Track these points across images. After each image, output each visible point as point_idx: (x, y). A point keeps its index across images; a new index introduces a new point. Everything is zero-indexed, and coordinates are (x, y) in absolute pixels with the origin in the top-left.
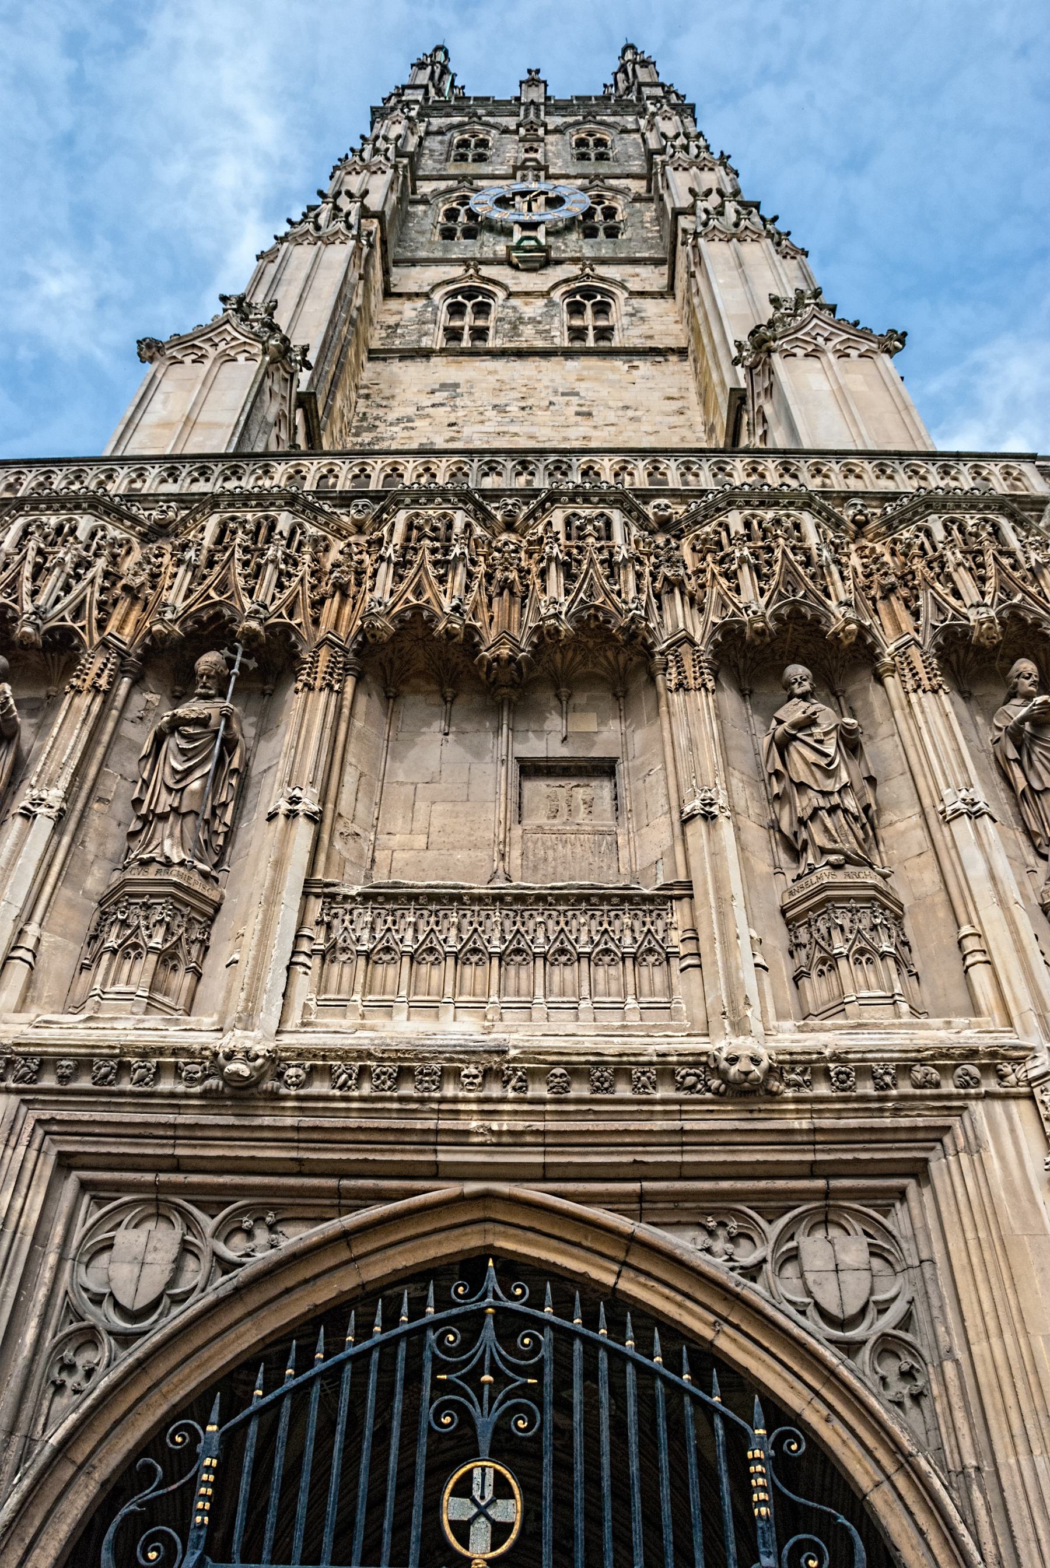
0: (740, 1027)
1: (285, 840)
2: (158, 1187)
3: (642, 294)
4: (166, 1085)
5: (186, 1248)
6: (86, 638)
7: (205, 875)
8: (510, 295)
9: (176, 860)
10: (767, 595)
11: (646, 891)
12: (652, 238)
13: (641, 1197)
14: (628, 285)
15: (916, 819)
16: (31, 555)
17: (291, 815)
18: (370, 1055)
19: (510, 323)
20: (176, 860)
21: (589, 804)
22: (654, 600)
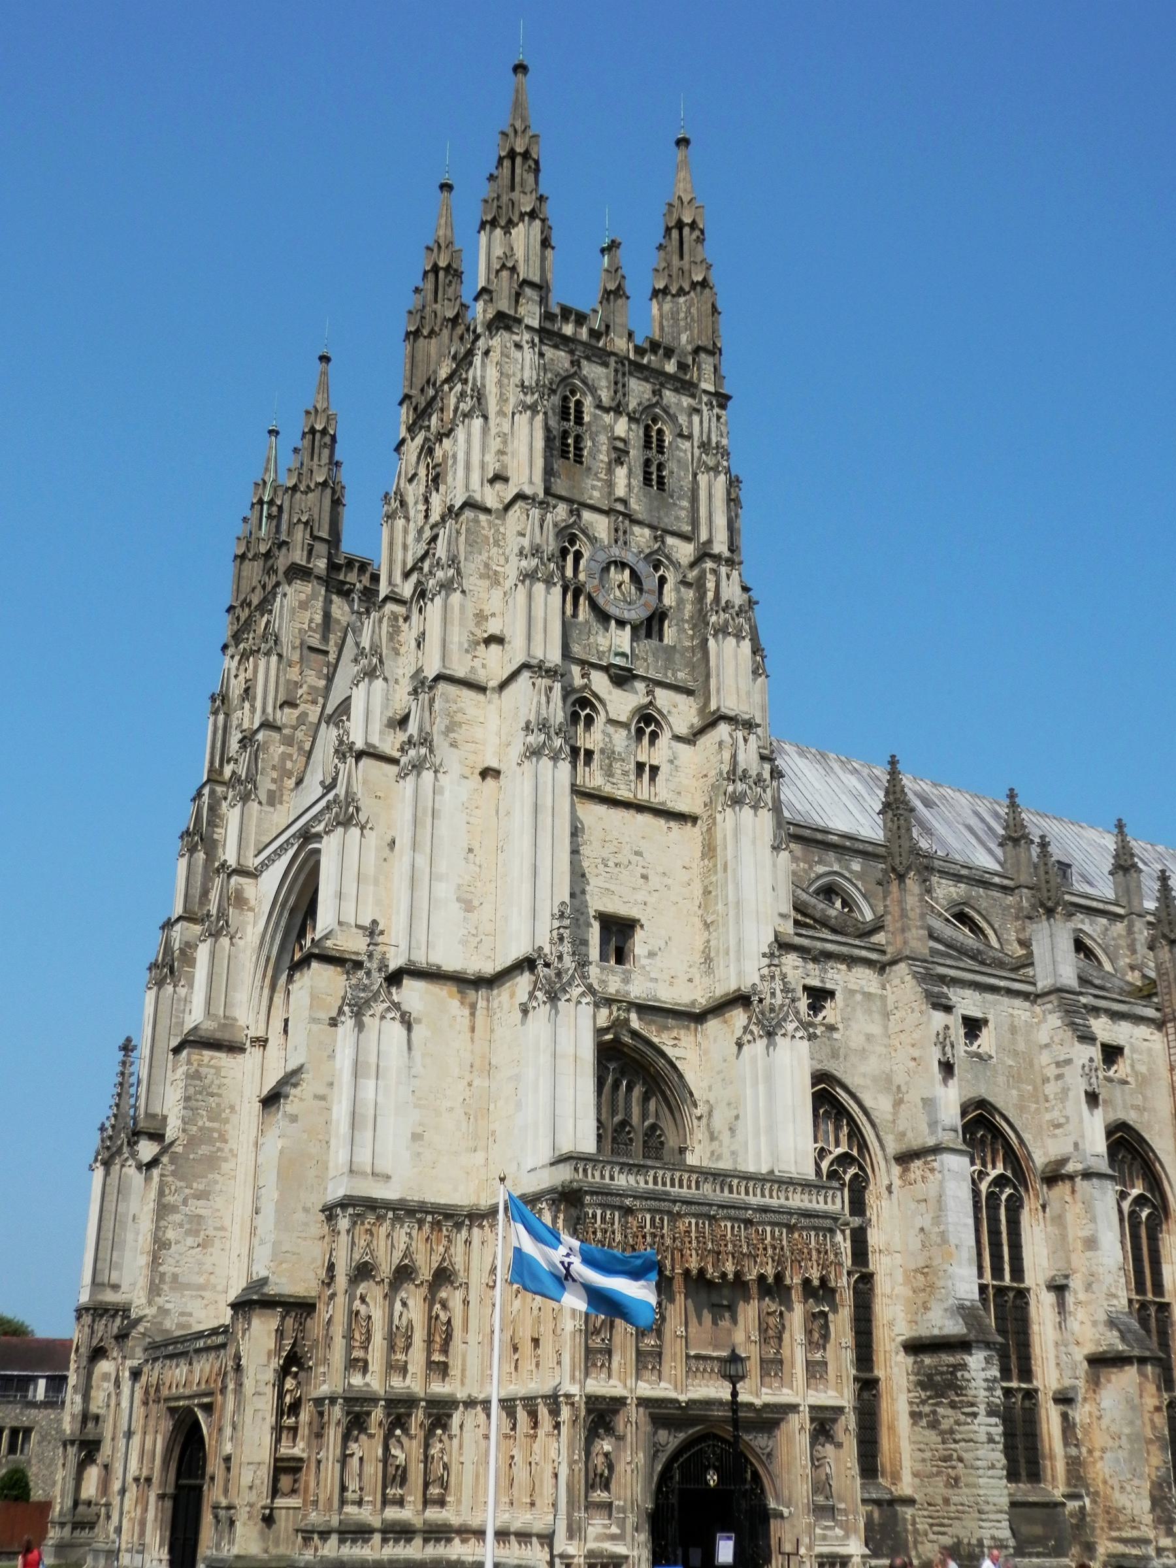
3: (677, 738)
8: (611, 721)
12: (687, 649)
14: (670, 719)
19: (609, 758)
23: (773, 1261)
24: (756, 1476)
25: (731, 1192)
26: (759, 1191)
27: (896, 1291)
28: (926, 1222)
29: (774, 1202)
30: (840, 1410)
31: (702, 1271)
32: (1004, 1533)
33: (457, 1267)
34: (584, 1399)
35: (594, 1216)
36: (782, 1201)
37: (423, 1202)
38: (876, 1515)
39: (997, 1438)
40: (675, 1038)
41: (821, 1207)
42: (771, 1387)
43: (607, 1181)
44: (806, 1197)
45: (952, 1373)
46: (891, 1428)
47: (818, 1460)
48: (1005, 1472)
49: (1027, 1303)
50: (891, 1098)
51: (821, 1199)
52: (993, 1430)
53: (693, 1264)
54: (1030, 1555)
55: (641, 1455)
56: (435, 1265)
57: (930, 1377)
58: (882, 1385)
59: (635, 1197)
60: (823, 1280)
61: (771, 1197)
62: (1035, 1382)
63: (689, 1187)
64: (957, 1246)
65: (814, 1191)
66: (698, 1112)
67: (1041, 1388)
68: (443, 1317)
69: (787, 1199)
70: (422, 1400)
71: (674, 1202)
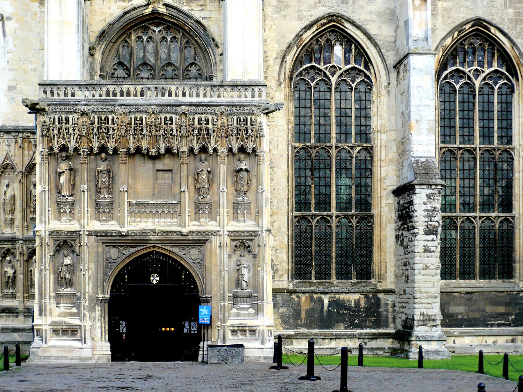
1: (124, 196)
11: (175, 202)
17: (124, 191)
21: (168, 177)
23: (199, 138)
24: (190, 276)
25: (170, 95)
26: (194, 94)
27: (390, 156)
28: (403, 107)
29: (206, 100)
31: (138, 150)
32: (435, 310)
34: (47, 233)
35: (54, 119)
38: (363, 303)
39: (432, 249)
40: (202, 5)
41: (249, 100)
42: (199, 221)
45: (408, 208)
46: (380, 246)
47: (239, 266)
48: (439, 271)
49: (512, 159)
50: (394, 26)
51: (249, 94)
52: (429, 244)
53: (132, 145)
54: (492, 325)
55: (93, 265)
57: (402, 211)
58: (376, 220)
60: (242, 150)
61: (205, 96)
62: (514, 212)
63: (136, 95)
64: (417, 121)
65: (242, 89)
66: (219, 51)
67: (517, 215)
69: (219, 96)
71: (121, 105)
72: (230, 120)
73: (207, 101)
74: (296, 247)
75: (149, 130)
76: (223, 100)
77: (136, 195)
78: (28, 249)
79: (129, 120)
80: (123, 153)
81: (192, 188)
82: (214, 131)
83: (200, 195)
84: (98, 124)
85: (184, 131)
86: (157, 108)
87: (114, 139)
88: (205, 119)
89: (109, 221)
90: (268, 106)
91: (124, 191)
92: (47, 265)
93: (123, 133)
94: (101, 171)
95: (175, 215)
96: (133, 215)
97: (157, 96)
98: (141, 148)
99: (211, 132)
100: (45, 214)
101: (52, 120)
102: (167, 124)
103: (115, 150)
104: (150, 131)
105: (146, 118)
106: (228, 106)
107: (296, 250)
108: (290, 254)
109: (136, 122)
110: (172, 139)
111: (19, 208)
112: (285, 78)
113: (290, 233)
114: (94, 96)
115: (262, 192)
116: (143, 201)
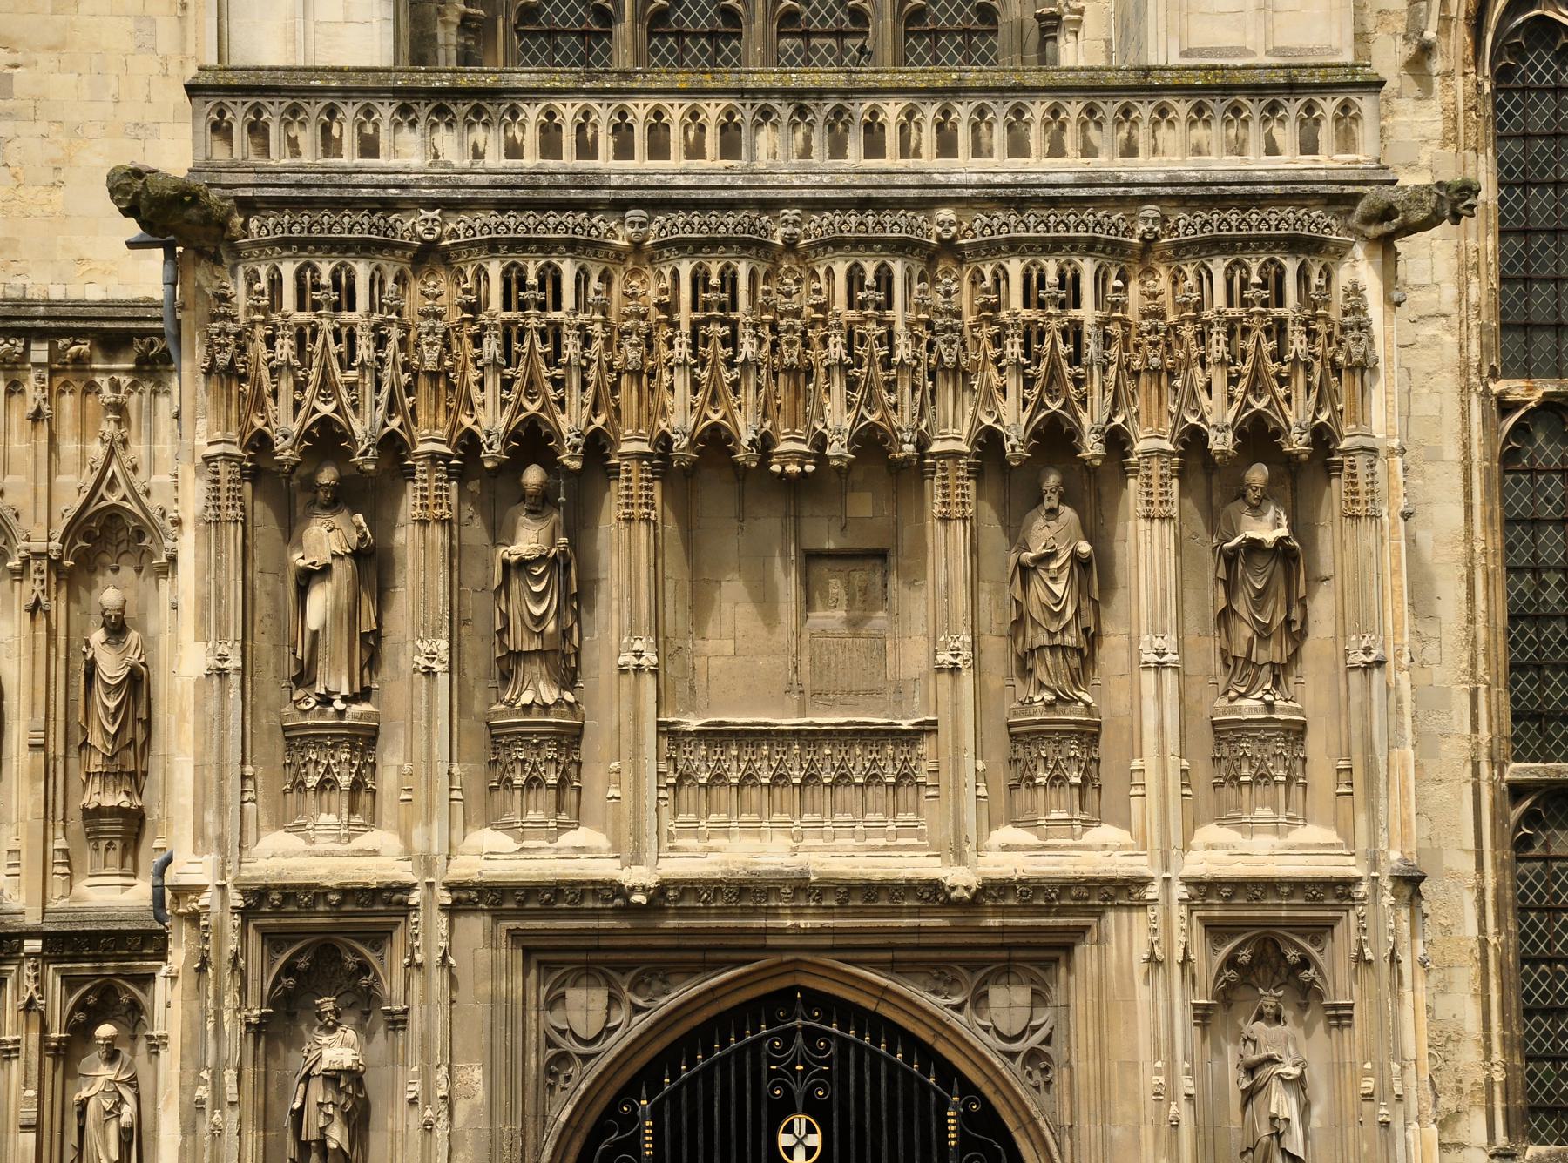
0: (959, 858)
1: (636, 694)
2: (587, 962)
4: (588, 904)
5: (611, 997)
6: (406, 437)
7: (569, 704)
9: (551, 702)
10: (1030, 408)
11: (905, 725)
13: (893, 961)
15: (1125, 638)
16: (330, 339)
18: (720, 881)
20: (551, 702)
22: (929, 384)
25: (874, 148)
26: (999, 136)
29: (1066, 168)
30: (1341, 889)
31: (715, 441)
33: (152, 504)
34: (236, 899)
36: (1107, 162)
37: (17, 304)
43: (349, 158)
44: (1213, 134)
56: (70, 502)
59: (450, 206)
61: (1057, 149)
68: (111, 666)
70: (32, 935)
71: (619, 206)
72: (1192, 281)
73: (1069, 178)
74: (1524, 961)
75: (769, 338)
76: (1148, 166)
77: (700, 683)
78: (70, 983)
79: (667, 284)
80: (634, 465)
81: (996, 649)
82: (1107, 340)
83: (1042, 686)
84: (507, 306)
85: (950, 343)
86: (817, 225)
87: (591, 390)
88: (1061, 276)
89: (562, 828)
90: (1387, 194)
91: (639, 669)
92: (230, 1076)
93: (631, 354)
94: (523, 565)
95: (907, 794)
96: (688, 794)
97: (806, 153)
98: (730, 438)
99: (1092, 348)
100: (221, 795)
101: (264, 284)
102: (863, 305)
103: (597, 446)
104: (775, 344)
105: (753, 275)
106: (1183, 201)
107: (1527, 976)
108: (1495, 997)
109: (703, 296)
110: (891, 386)
111: (26, 756)
112: (1446, 20)
113: (1490, 883)
114: (478, 154)
115: (1367, 668)
116: (739, 718)
